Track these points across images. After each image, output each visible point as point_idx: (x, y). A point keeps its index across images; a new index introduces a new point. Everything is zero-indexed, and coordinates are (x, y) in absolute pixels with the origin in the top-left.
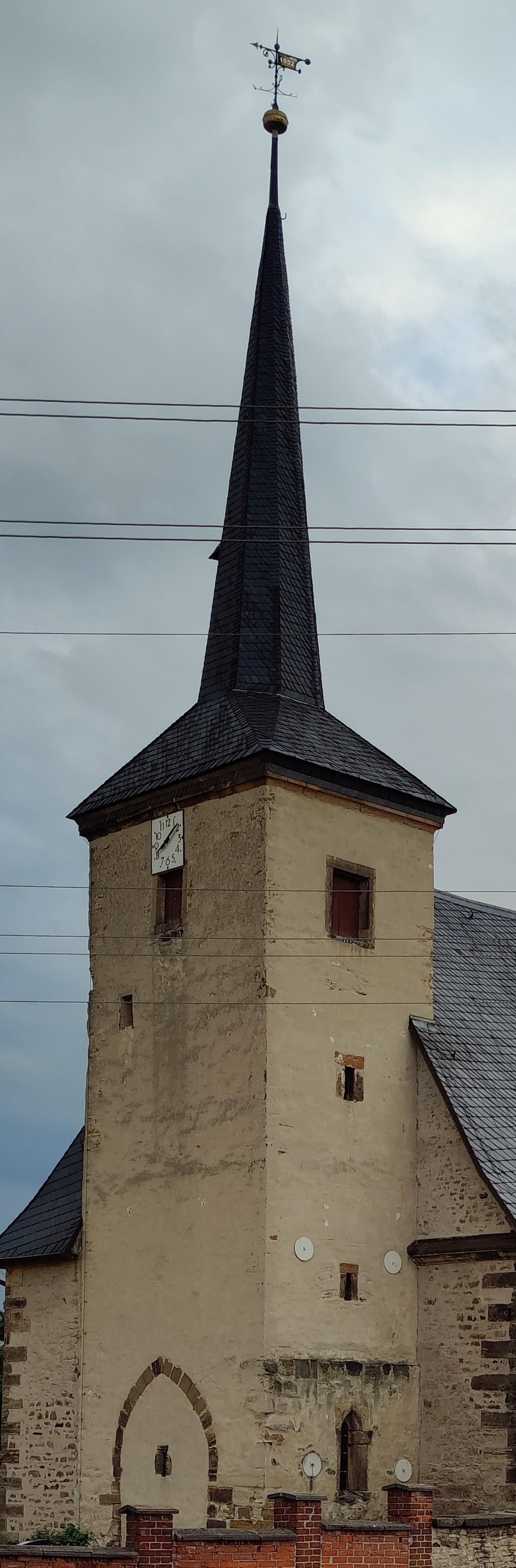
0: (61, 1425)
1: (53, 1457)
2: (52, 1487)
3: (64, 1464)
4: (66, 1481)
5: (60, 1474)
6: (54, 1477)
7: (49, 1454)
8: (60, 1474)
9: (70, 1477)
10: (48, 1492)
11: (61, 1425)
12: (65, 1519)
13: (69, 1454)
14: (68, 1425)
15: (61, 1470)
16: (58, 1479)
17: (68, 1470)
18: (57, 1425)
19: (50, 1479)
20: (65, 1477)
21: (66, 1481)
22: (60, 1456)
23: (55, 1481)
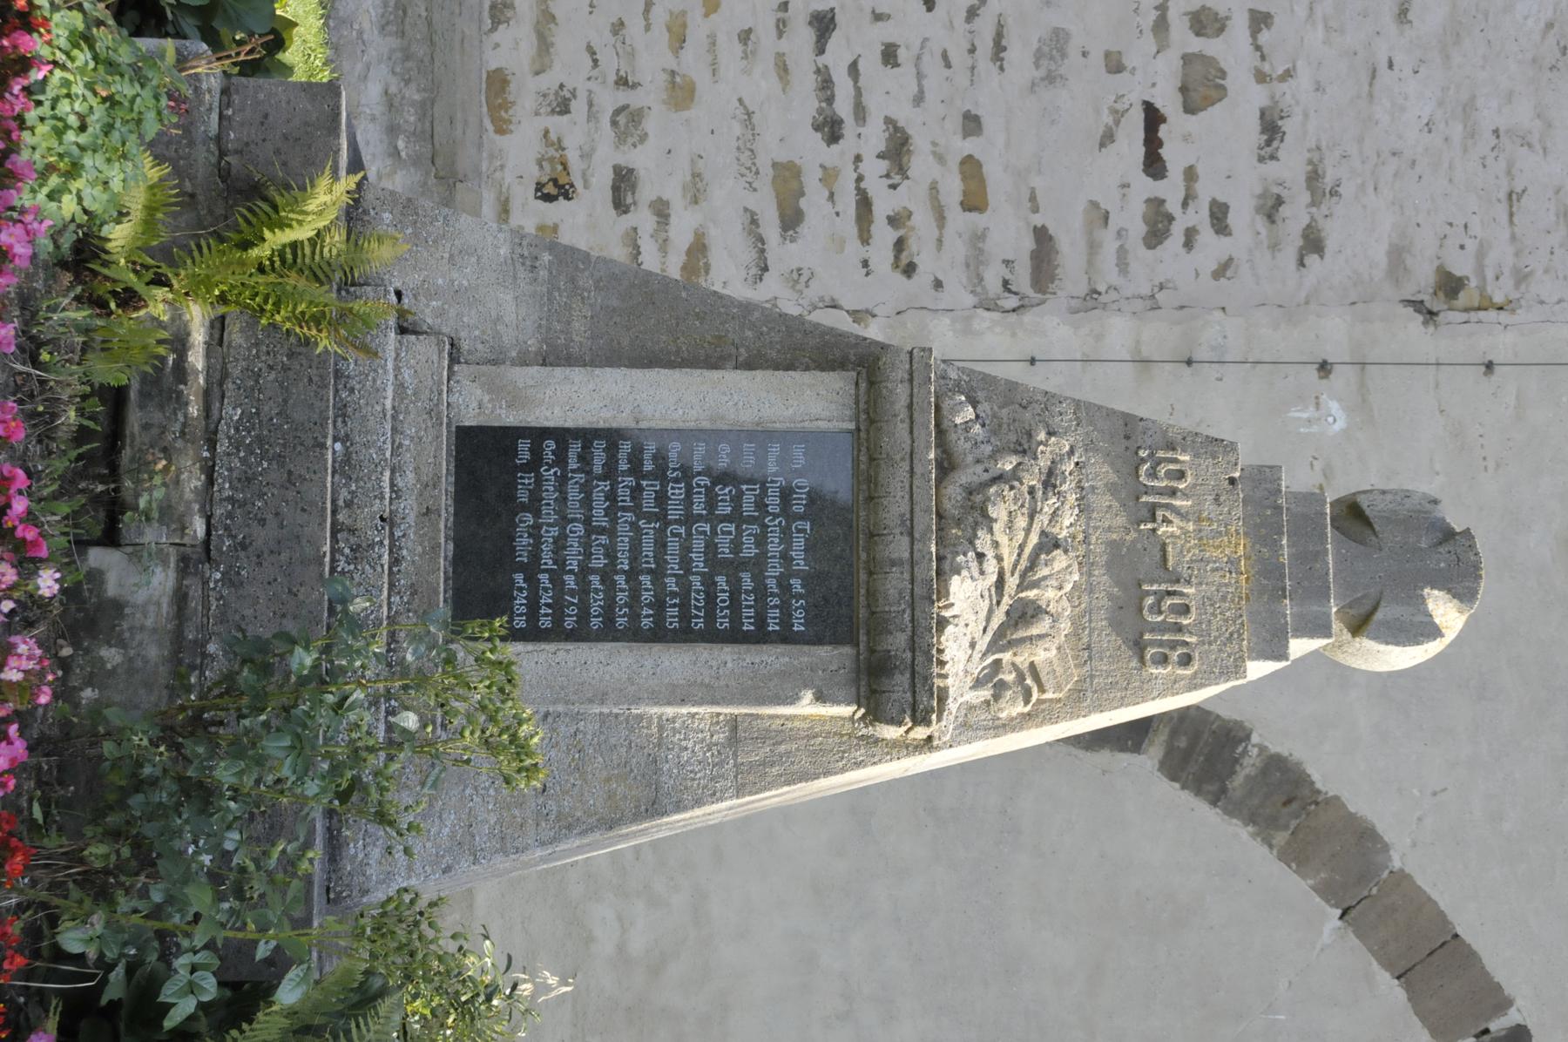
0: (1154, 164)
1: (994, 94)
2: (826, 84)
3: (953, 188)
4: (864, 203)
5: (898, 148)
6: (889, 95)
7: (999, 48)
8: (898, 148)
9: (885, 237)
10: (804, 36)
11: (1154, 164)
12: (661, 211)
13: (1008, 236)
14: (1158, 226)
15: (921, 164)
16: (874, 138)
17: (922, 220)
18: (1153, 118)
19: (871, 64)
20: (884, 204)
21: (864, 203)
22: (990, 150)
23: (860, 112)
